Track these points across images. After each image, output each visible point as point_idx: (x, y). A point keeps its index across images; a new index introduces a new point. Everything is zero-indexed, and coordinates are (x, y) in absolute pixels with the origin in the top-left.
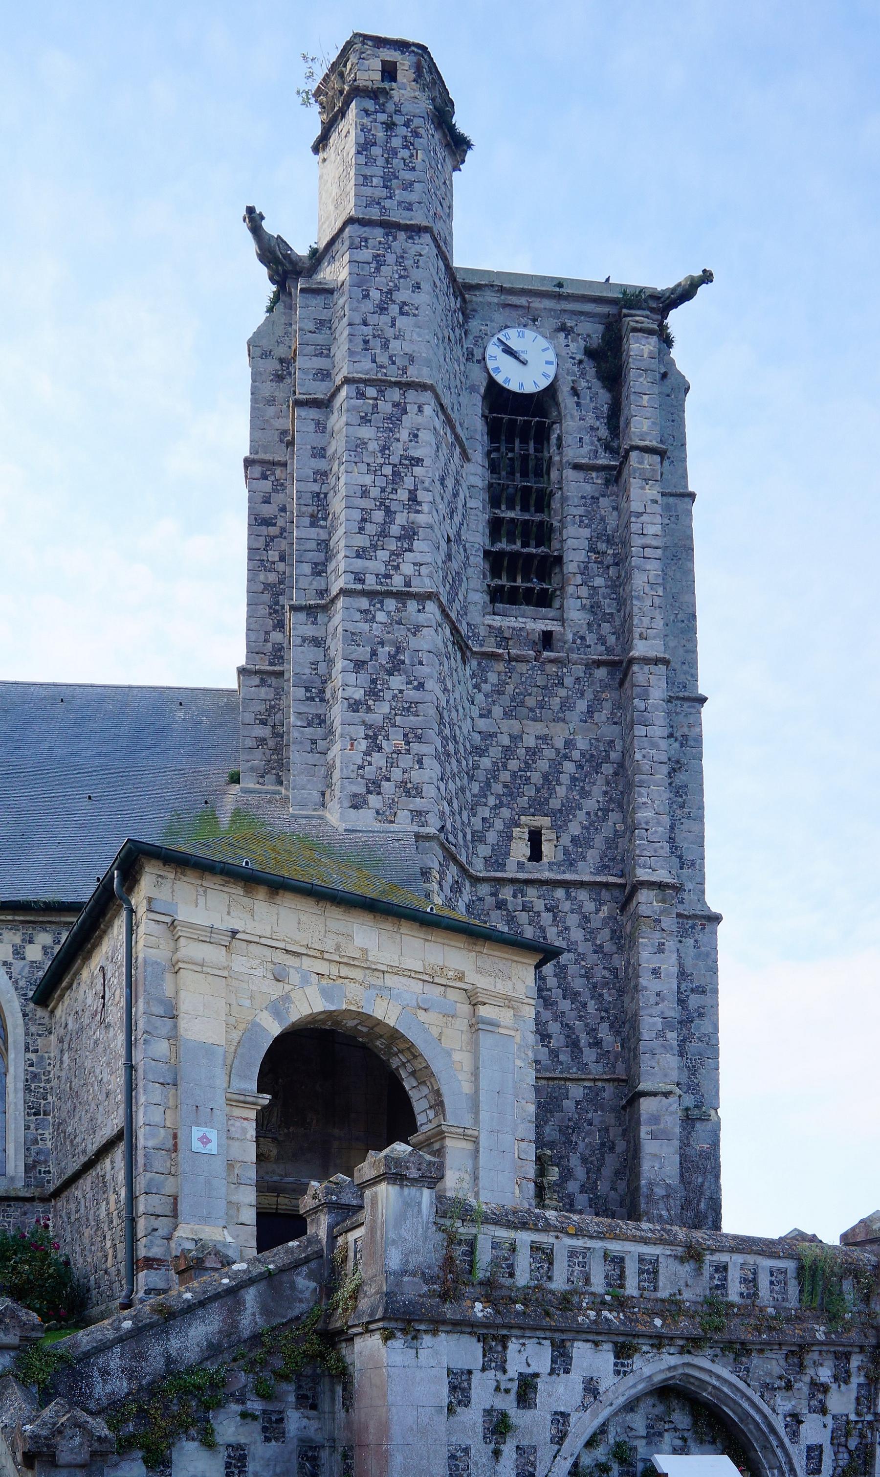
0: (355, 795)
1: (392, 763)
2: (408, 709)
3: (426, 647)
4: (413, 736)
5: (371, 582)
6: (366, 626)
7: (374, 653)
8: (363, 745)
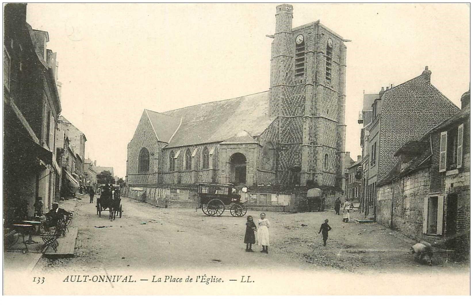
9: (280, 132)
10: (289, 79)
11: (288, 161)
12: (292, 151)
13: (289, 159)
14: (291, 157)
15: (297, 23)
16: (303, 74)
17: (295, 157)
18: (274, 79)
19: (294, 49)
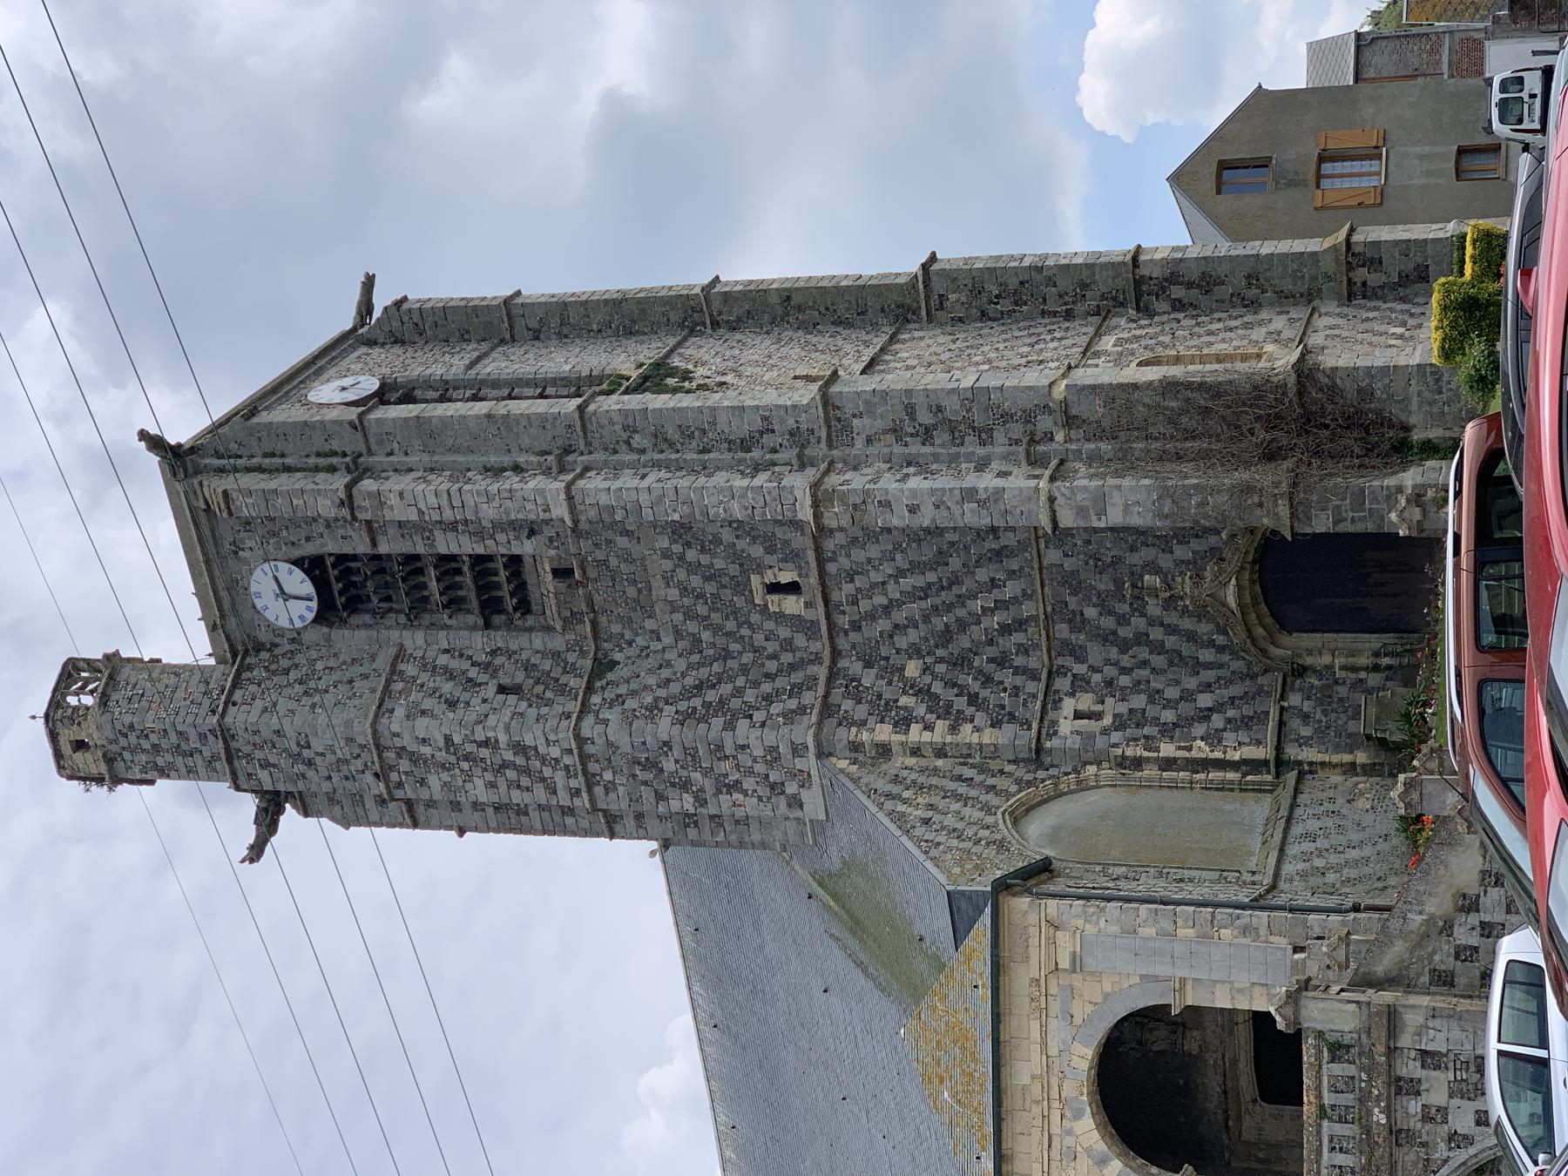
0: (789, 806)
1: (750, 772)
2: (693, 757)
3: (627, 738)
4: (717, 750)
6: (621, 789)
7: (645, 783)
8: (736, 796)
10: (544, 679)
12: (1108, 638)
13: (1176, 659)
14: (1159, 648)
16: (515, 561)
17: (1153, 608)
18: (540, 793)
19: (351, 638)
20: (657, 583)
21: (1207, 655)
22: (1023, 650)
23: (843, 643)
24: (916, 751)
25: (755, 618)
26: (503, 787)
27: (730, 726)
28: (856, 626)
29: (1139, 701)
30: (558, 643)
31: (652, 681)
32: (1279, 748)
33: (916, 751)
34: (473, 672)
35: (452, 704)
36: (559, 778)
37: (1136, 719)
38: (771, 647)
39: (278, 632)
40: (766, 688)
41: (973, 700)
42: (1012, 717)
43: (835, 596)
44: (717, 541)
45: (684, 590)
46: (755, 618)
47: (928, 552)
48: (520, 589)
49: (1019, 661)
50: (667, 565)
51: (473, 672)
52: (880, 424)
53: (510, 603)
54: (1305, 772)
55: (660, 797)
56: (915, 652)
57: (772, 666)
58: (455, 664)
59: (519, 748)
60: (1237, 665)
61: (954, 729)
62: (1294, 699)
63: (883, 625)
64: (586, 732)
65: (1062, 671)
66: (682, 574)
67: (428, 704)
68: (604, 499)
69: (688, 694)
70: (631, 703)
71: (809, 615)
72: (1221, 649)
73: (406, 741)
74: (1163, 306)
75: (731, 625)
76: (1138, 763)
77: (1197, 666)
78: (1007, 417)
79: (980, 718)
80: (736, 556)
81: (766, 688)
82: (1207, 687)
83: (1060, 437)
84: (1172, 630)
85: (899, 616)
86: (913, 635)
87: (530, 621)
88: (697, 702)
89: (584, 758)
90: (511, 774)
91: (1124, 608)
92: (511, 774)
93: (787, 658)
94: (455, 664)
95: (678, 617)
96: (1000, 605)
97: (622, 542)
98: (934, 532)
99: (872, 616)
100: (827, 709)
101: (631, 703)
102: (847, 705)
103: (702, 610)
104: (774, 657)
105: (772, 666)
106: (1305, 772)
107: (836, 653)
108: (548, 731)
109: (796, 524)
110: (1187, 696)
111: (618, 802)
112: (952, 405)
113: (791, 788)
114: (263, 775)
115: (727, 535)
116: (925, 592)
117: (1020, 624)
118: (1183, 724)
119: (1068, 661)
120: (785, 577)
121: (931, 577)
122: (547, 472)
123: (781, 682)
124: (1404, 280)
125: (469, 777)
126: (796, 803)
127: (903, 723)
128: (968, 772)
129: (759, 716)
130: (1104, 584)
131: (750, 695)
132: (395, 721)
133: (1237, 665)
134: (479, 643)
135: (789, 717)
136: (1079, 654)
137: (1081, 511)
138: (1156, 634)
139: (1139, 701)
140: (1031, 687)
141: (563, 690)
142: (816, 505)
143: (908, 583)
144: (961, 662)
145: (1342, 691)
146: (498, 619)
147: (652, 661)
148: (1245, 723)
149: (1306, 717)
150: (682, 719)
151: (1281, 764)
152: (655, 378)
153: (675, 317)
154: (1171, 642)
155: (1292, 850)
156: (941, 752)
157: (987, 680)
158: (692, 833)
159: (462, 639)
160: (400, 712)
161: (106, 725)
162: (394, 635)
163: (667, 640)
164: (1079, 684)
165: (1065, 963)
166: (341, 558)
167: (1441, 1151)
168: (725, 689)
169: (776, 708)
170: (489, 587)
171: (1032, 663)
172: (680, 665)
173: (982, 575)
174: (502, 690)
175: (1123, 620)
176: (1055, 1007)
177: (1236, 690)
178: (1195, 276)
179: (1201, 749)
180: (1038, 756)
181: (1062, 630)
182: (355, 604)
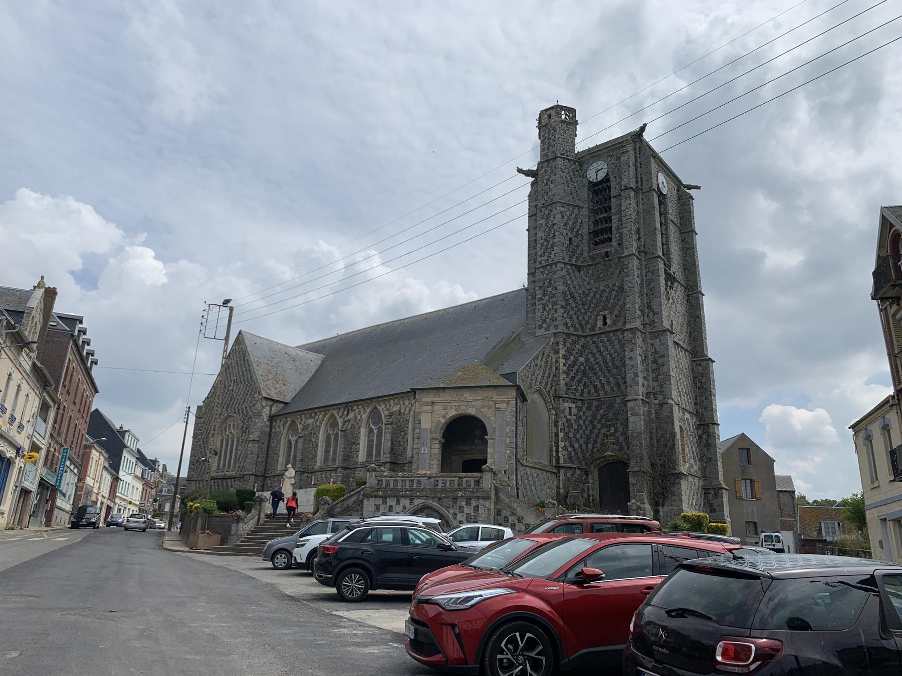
5: (544, 264)
9: (563, 368)
11: (587, 444)
13: (588, 437)
14: (591, 432)
15: (586, 139)
16: (610, 240)
17: (604, 430)
18: (540, 253)
19: (585, 193)
20: (605, 283)
21: (590, 446)
22: (589, 392)
23: (588, 339)
24: (557, 361)
25: (595, 313)
26: (542, 241)
27: (562, 307)
28: (594, 342)
29: (575, 426)
30: (585, 254)
31: (575, 283)
32: (563, 467)
33: (557, 361)
34: (575, 230)
35: (566, 224)
36: (545, 258)
37: (570, 426)
38: (587, 318)
39: (586, 171)
40: (574, 317)
41: (573, 378)
42: (568, 389)
43: (603, 336)
44: (619, 300)
45: (603, 291)
46: (595, 313)
47: (617, 363)
48: (602, 242)
49: (586, 391)
50: (611, 286)
51: (575, 230)
52: (658, 348)
53: (597, 239)
54: (557, 475)
55: (540, 287)
56: (587, 360)
57: (581, 318)
58: (578, 224)
59: (553, 245)
60: (587, 455)
61: (564, 372)
62: (578, 472)
63: (595, 350)
64: (559, 265)
65: (583, 403)
66: (608, 290)
67: (565, 217)
68: (630, 265)
69: (571, 294)
70: (568, 277)
71: (597, 329)
72: (592, 451)
73: (554, 212)
74: (700, 432)
75: (593, 305)
76: (556, 426)
77: (587, 444)
78: (661, 386)
79: (568, 380)
80: (614, 306)
81: (574, 317)
82: (580, 446)
83: (656, 402)
84: (597, 436)
85: (597, 355)
86: (592, 359)
87: (592, 246)
88: (569, 297)
89: (551, 265)
90: (545, 244)
91: (603, 421)
92: (545, 244)
93: (583, 322)
94: (578, 224)
95: (595, 290)
96: (602, 385)
97: (617, 272)
98: (624, 365)
99: (597, 347)
100: (568, 335)
101: (568, 277)
102: (570, 341)
103: (597, 297)
104: (584, 319)
105: (581, 318)
106: (557, 475)
107: (585, 337)
108: (558, 254)
109: (625, 323)
110: (577, 440)
111: (539, 276)
112: (665, 369)
113: (545, 326)
114: (543, 171)
115: (620, 303)
116: (605, 362)
117: (597, 391)
118: (569, 439)
119: (586, 405)
120: (608, 321)
121: (610, 364)
122: (638, 248)
123: (576, 321)
124: (711, 505)
125: (544, 231)
126: (540, 327)
127: (565, 357)
128: (551, 377)
129: (565, 315)
130: (610, 416)
131: (572, 312)
132: (560, 208)
133: (587, 455)
134: (585, 231)
135: (566, 324)
136: (588, 409)
137: (633, 409)
138: (596, 431)
139: (575, 426)
140: (578, 394)
141: (571, 257)
142: (631, 329)
143: (608, 358)
144: (584, 373)
145: (581, 485)
146: (592, 236)
147: (581, 283)
148: (570, 457)
149: (573, 475)
150: (564, 293)
151: (559, 468)
152: (670, 278)
153: (690, 283)
154: (594, 435)
155: (533, 471)
156: (557, 368)
157: (579, 382)
158: (530, 297)
159: (585, 226)
160: (563, 209)
161: (556, 123)
162: (586, 205)
163: (587, 287)
164: (579, 409)
165: (497, 406)
166: (609, 187)
167: (452, 511)
168: (573, 305)
169: (568, 320)
170: (602, 233)
171: (585, 395)
172: (580, 291)
173: (611, 379)
174: (571, 239)
175: (599, 421)
176: (485, 403)
177: (580, 455)
178: (710, 442)
179: (562, 444)
180: (557, 397)
181: (595, 403)
182: (595, 193)
